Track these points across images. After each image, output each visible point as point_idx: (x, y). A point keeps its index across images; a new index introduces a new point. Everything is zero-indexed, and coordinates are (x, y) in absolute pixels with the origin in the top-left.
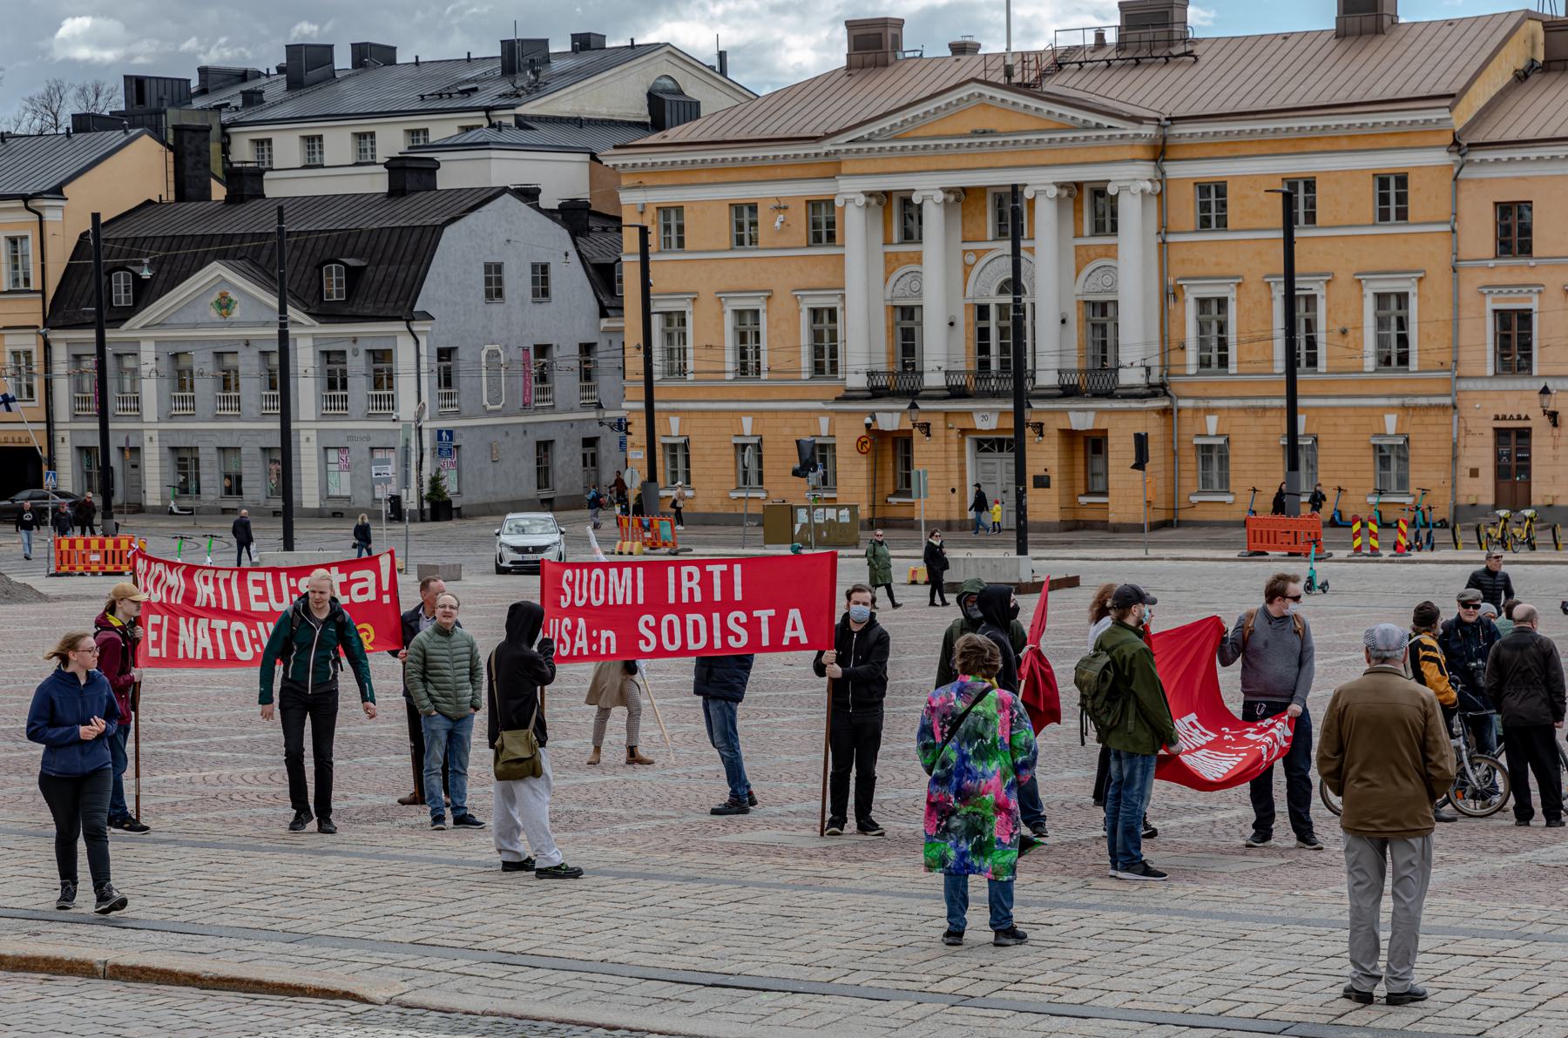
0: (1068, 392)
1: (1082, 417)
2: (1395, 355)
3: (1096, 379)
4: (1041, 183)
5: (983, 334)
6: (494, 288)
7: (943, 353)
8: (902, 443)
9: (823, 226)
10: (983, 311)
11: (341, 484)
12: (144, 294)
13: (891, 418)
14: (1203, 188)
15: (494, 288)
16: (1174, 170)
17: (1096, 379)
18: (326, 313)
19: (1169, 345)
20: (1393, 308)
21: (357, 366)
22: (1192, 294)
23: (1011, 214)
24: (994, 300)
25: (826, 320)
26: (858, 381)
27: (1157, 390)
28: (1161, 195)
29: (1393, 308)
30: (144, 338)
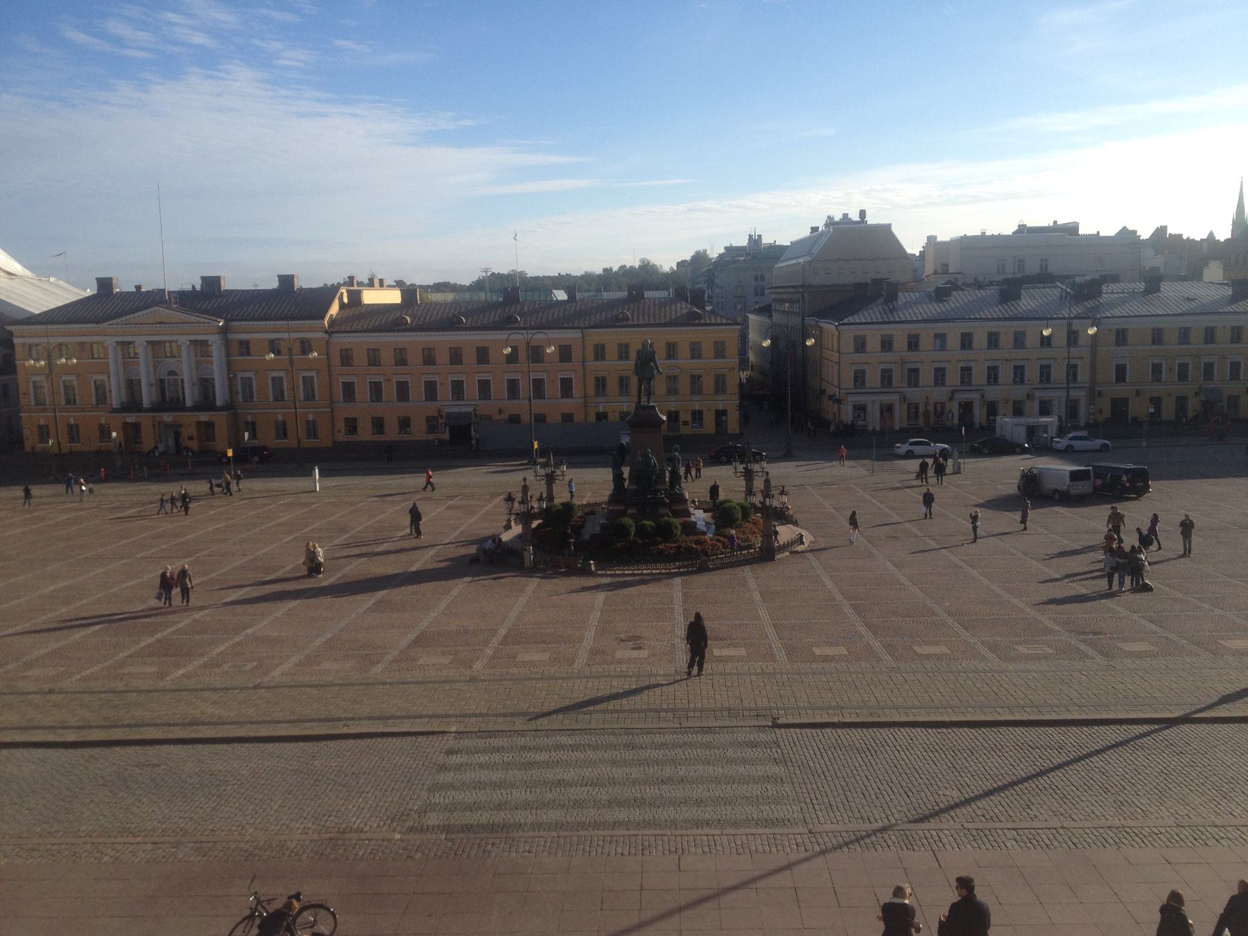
0: (197, 408)
1: (204, 417)
2: (310, 396)
3: (206, 402)
5: (163, 390)
7: (147, 396)
10: (162, 381)
16: (231, 336)
20: (308, 382)
22: (241, 375)
24: (166, 377)
26: (115, 403)
27: (229, 407)
28: (227, 343)
29: (308, 382)
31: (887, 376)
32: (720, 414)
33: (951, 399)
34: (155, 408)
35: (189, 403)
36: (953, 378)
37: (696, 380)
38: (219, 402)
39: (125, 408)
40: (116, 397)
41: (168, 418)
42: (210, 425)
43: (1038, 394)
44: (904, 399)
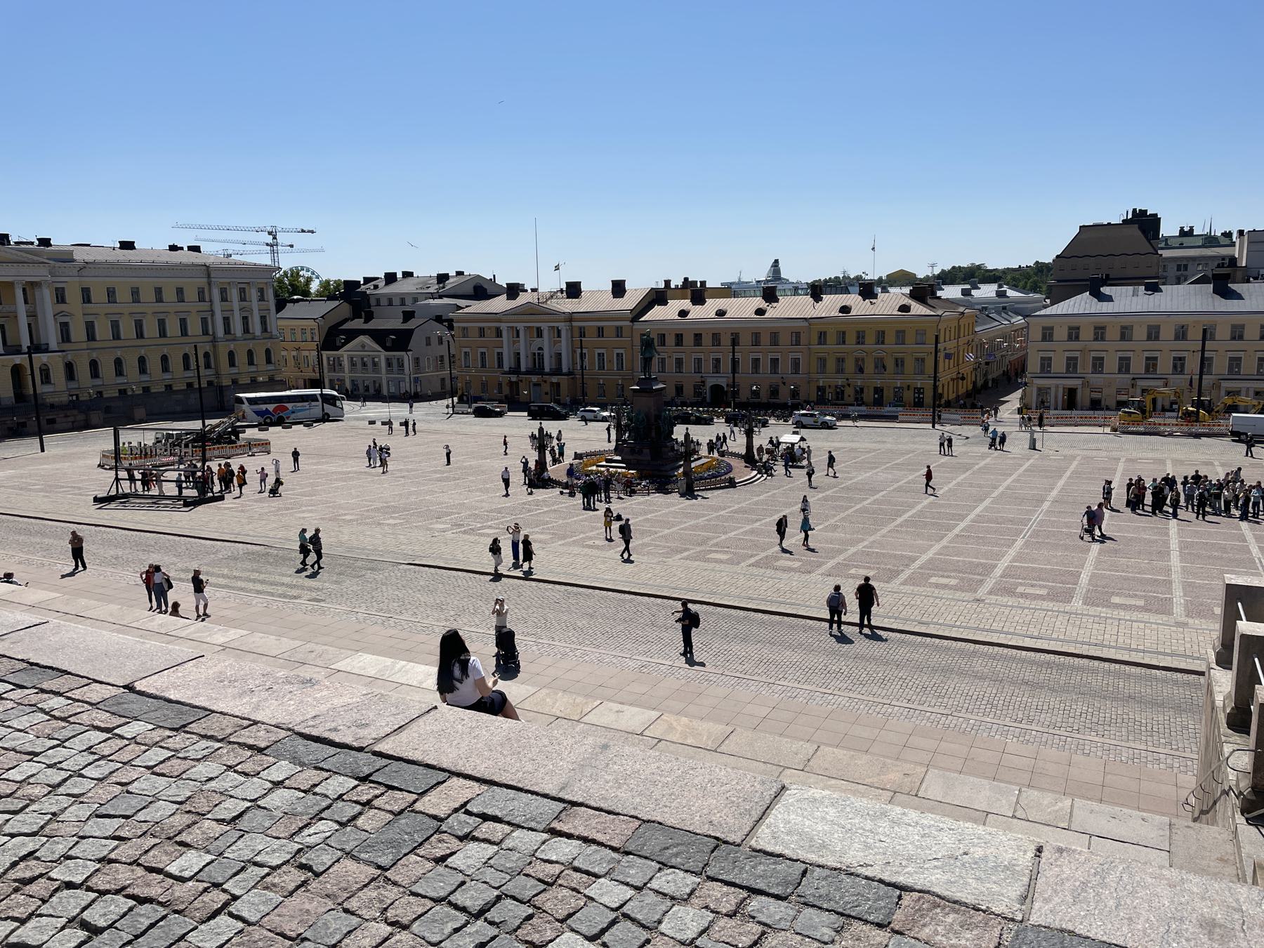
1: (555, 379)
3: (557, 371)
4: (544, 326)
6: (428, 343)
8: (517, 383)
9: (499, 333)
11: (393, 390)
12: (347, 341)
13: (514, 378)
14: (580, 328)
15: (428, 343)
16: (574, 324)
17: (557, 371)
18: (387, 349)
19: (574, 363)
21: (395, 362)
23: (539, 333)
25: (500, 355)
26: (506, 368)
27: (570, 373)
30: (344, 354)
31: (1072, 363)
32: (919, 391)
33: (1133, 386)
34: (527, 373)
35: (547, 369)
36: (1138, 366)
37: (899, 363)
38: (565, 370)
39: (509, 373)
40: (507, 364)
41: (535, 379)
42: (558, 384)
43: (1225, 384)
44: (1086, 384)
